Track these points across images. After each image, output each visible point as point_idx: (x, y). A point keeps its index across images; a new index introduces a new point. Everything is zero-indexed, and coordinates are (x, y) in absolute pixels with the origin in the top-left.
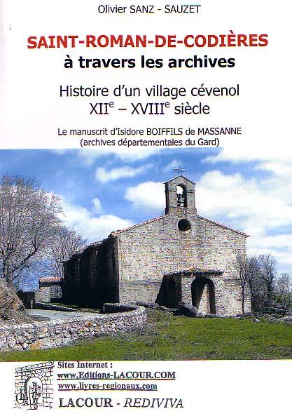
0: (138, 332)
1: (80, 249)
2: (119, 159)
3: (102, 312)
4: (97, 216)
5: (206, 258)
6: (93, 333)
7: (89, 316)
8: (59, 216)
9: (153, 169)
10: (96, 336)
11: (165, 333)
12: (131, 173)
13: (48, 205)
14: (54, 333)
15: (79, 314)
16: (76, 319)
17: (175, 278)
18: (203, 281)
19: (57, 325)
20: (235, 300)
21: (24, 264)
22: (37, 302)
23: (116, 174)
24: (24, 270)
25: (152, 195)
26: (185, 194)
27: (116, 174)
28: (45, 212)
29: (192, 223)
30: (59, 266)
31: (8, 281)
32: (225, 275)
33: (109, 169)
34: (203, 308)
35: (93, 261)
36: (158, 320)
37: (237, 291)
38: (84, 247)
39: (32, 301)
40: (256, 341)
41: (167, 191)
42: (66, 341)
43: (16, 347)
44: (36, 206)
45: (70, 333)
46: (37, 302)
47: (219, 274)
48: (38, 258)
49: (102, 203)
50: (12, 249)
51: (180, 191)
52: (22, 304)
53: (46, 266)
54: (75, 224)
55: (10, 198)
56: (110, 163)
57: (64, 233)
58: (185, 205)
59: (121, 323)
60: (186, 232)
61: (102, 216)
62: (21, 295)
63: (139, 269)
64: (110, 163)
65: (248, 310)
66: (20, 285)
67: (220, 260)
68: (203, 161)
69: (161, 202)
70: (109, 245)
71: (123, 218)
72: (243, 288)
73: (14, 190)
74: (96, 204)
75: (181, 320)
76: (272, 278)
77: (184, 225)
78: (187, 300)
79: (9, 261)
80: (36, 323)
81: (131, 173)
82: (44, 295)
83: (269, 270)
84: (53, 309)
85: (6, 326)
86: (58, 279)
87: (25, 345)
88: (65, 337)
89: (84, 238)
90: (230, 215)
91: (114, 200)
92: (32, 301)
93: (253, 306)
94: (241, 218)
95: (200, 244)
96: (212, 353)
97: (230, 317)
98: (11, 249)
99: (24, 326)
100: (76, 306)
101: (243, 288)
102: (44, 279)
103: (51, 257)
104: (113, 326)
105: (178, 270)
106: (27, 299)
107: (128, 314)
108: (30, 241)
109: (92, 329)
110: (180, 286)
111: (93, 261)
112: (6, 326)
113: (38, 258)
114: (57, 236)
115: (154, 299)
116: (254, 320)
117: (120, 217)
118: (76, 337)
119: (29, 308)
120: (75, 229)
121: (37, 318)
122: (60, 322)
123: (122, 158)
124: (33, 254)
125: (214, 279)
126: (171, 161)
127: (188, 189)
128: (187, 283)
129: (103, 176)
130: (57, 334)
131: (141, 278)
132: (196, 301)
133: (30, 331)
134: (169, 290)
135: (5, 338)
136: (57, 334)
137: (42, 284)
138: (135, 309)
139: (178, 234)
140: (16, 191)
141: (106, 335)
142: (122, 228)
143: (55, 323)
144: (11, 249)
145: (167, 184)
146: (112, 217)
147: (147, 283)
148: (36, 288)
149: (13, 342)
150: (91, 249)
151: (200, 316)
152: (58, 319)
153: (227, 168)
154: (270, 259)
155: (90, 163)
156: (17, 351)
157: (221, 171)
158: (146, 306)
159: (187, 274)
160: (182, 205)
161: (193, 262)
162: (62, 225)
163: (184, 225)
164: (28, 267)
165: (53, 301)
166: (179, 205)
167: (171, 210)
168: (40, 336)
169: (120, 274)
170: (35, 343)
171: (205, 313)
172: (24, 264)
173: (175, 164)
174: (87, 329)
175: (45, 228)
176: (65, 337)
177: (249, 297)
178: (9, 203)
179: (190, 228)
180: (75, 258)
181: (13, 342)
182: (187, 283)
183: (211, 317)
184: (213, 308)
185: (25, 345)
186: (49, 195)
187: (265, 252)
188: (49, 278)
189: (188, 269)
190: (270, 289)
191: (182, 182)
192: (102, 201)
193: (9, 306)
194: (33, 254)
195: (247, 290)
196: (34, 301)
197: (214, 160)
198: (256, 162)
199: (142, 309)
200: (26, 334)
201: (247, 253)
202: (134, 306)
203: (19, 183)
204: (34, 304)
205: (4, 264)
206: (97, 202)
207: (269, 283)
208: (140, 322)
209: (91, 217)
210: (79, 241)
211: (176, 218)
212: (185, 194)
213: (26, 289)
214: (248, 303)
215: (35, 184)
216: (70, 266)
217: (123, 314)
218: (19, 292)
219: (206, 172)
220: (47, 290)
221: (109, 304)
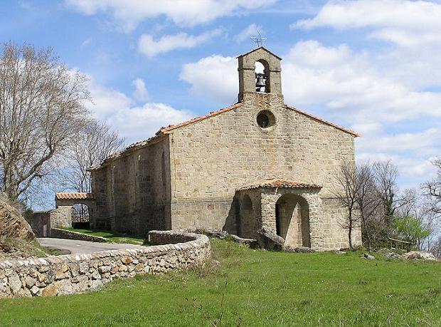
0: (196, 271)
1: (115, 151)
2: (172, 23)
3: (146, 243)
4: (141, 105)
5: (297, 166)
6: (133, 273)
7: (131, 248)
8: (86, 104)
9: (216, 34)
10: (138, 277)
11: (235, 275)
12: (190, 43)
13: (69, 87)
14: (75, 273)
15: (114, 245)
16: (109, 252)
17: (251, 195)
18: (292, 200)
19: (82, 261)
20: (338, 228)
21: (36, 171)
22: (52, 227)
23: (167, 44)
24: (35, 181)
25: (221, 74)
26: (266, 74)
27: (167, 44)
28: (65, 99)
29: (278, 116)
30: (85, 175)
31: (10, 197)
32: (325, 192)
33: (157, 38)
34: (292, 238)
35: (134, 168)
36: (227, 256)
37: (341, 216)
38: (122, 148)
39: (45, 227)
40: (368, 287)
41: (241, 70)
42: (94, 285)
43: (22, 292)
44: (51, 88)
45: (101, 273)
46: (52, 227)
47: (316, 189)
48: (55, 165)
49: (146, 86)
50: (17, 150)
51: (260, 68)
52: (31, 231)
53: (63, 179)
54: (110, 114)
55: (16, 77)
56: (159, 27)
57: (93, 130)
58: (268, 90)
59: (174, 259)
60: (268, 129)
61: (148, 104)
62: (32, 217)
63: (201, 182)
64: (159, 27)
65: (357, 239)
66: (29, 204)
67: (318, 169)
68: (292, 26)
69: (230, 80)
70: (159, 144)
71: (177, 107)
72: (350, 210)
73: (21, 65)
74: (139, 87)
75: (262, 255)
76: (392, 195)
77: (265, 119)
78: (269, 226)
79: (13, 167)
80: (52, 258)
81: (190, 43)
82: (63, 218)
83: (388, 184)
84: (75, 237)
85: (7, 262)
86: (83, 195)
87: (35, 290)
88: (93, 279)
89: (120, 136)
90: (333, 104)
91: (165, 82)
92: (45, 227)
93: (365, 236)
94: (349, 109)
95: (288, 143)
96: (305, 303)
97: (332, 252)
98: (15, 151)
99: (33, 262)
100: (109, 234)
101: (350, 210)
102: (61, 195)
103: (74, 162)
104: (163, 263)
105: (256, 184)
106: (39, 222)
107: (185, 245)
108: (43, 140)
109: (131, 268)
110: (259, 205)
111: (134, 168)
112: (7, 262)
113: (55, 165)
114: (81, 134)
115: (221, 223)
116: (367, 257)
117: (173, 107)
118: (109, 278)
119: (40, 235)
120: (109, 122)
121: (51, 251)
122: (86, 256)
123: (177, 20)
124: (47, 158)
125: (308, 196)
126: (245, 27)
127: (272, 67)
128: (269, 203)
129: (149, 46)
130: (82, 274)
131: (202, 195)
132: (280, 229)
133: (43, 269)
134: (243, 208)
135: (5, 280)
136: (82, 274)
137: (61, 202)
138: (194, 239)
139: (254, 129)
140: (23, 66)
141: (152, 277)
142: (175, 123)
143: (78, 258)
144: (15, 151)
145: (240, 58)
146: (161, 106)
147: (211, 204)
148: (52, 208)
149: (17, 284)
150: (130, 152)
151: (289, 250)
152: (82, 252)
153: (327, 36)
154: (389, 169)
155: (130, 27)
156: (24, 298)
157: (319, 41)
158: (209, 235)
159: (270, 189)
160: (263, 89)
161: (279, 173)
162: (89, 117)
163: (265, 119)
164: (40, 176)
165: (77, 226)
166: (258, 90)
167: (247, 96)
168: (57, 277)
169: (173, 188)
170: (49, 287)
171: (293, 246)
172: (36, 171)
173: (252, 30)
174: (125, 267)
175: (62, 122)
176: (93, 279)
177: (357, 224)
178: (15, 85)
179: (274, 123)
180: (107, 164)
181: (17, 284)
182: (269, 203)
183: (303, 251)
184: (306, 238)
185: (35, 290)
186: (71, 74)
187: (383, 158)
188: (71, 193)
189: (271, 182)
190: (389, 212)
191: (264, 56)
192: (147, 82)
193: (12, 233)
194: (47, 158)
195: (356, 214)
196: (49, 227)
197: (308, 24)
198: (370, 29)
199: (204, 239)
200: (37, 273)
201: (356, 160)
202: (193, 235)
203: (28, 56)
204: (48, 230)
205: (6, 172)
206: (140, 84)
207: (387, 202)
208: (201, 257)
209: (132, 107)
210: (112, 141)
211: (252, 108)
212: (266, 74)
213: (37, 209)
214: (357, 233)
215: (50, 58)
216: (101, 174)
217: (177, 246)
218: (26, 213)
219: (296, 42)
220: (66, 210)
221: (157, 232)
